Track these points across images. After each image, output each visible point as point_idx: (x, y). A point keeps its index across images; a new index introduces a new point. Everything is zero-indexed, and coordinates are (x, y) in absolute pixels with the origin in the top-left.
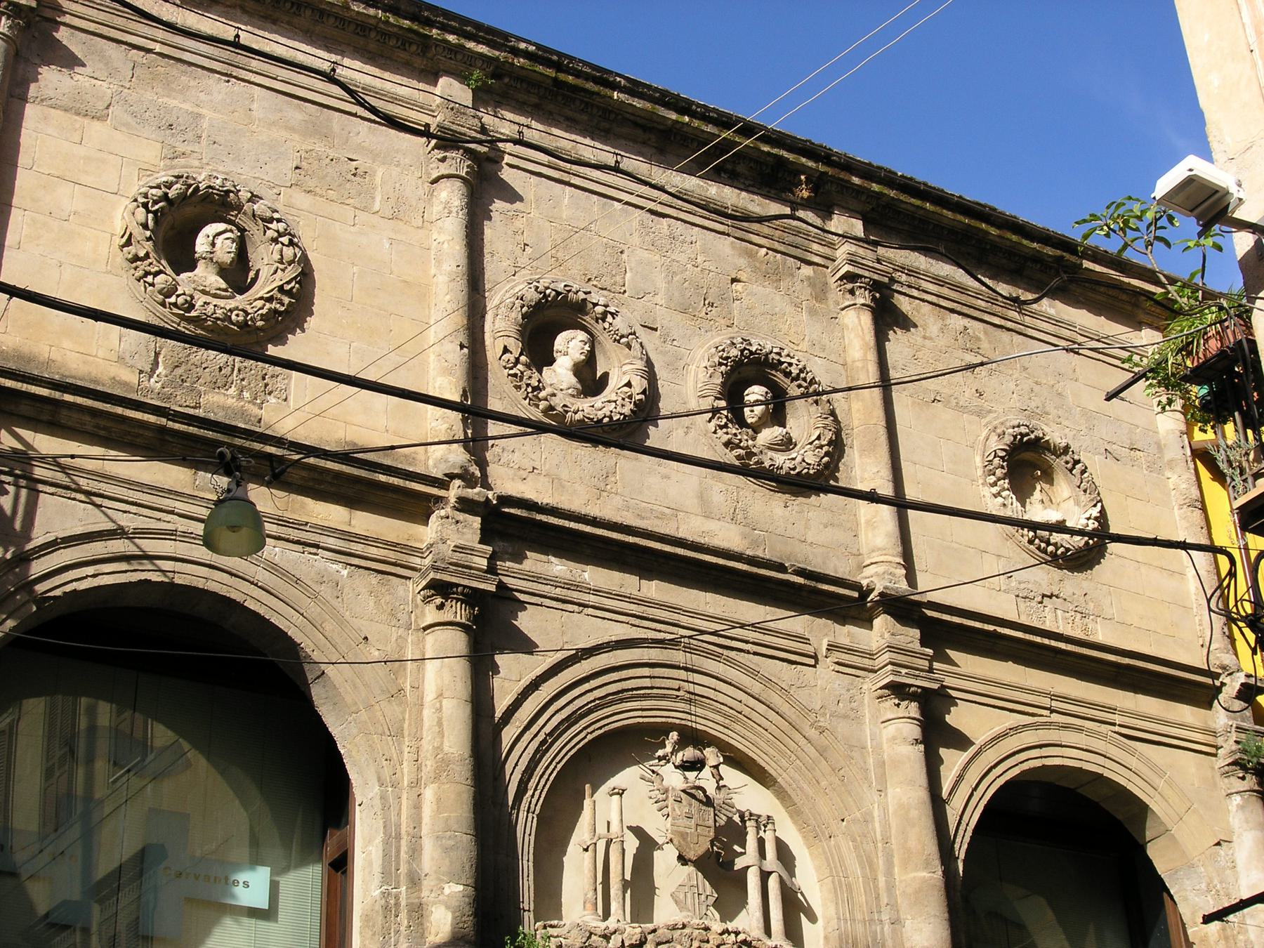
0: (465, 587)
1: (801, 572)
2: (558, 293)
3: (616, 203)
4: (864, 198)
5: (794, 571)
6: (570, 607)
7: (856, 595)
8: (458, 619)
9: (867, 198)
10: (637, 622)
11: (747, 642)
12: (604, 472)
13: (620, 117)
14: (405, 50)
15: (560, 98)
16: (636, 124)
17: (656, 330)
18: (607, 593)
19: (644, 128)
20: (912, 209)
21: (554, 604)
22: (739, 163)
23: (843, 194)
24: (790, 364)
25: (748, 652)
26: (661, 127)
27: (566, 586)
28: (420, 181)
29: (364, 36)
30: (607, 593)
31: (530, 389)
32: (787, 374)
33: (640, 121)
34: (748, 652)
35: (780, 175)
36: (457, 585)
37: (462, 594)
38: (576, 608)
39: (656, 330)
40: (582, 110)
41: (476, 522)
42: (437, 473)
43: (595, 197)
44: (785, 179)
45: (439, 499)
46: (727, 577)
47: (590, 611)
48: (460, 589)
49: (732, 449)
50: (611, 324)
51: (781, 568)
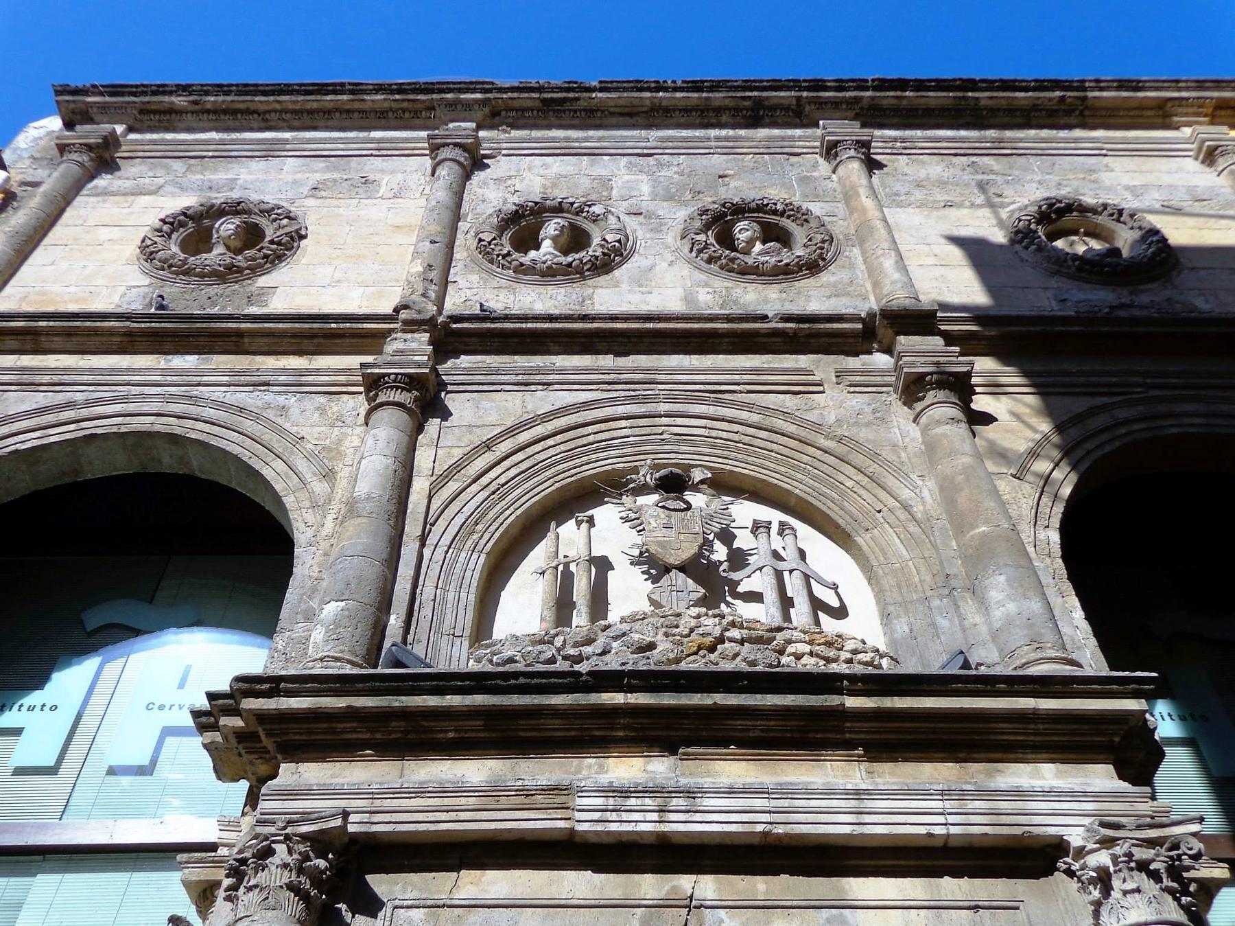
0: (397, 374)
1: (787, 318)
2: (536, 203)
3: (605, 157)
4: (844, 106)
5: (781, 318)
6: (533, 388)
7: (860, 326)
8: (391, 399)
9: (847, 105)
10: (609, 387)
11: (738, 384)
12: (581, 300)
13: (606, 113)
14: (418, 118)
15: (551, 113)
16: (622, 115)
17: (641, 214)
18: (573, 370)
19: (630, 115)
20: (894, 102)
21: (516, 388)
22: (721, 116)
23: (822, 108)
24: (776, 204)
25: (741, 392)
26: (645, 109)
27: (527, 372)
28: (423, 177)
29: (384, 118)
30: (573, 370)
31: (500, 258)
32: (775, 212)
33: (626, 110)
34: (741, 392)
35: (761, 113)
36: (389, 375)
37: (395, 381)
38: (540, 387)
39: (641, 214)
40: (573, 117)
41: (425, 337)
42: (388, 310)
43: (585, 157)
44: (767, 115)
45: (390, 331)
46: (711, 341)
47: (556, 387)
48: (392, 377)
49: (716, 262)
50: (588, 212)
51: (764, 318)
